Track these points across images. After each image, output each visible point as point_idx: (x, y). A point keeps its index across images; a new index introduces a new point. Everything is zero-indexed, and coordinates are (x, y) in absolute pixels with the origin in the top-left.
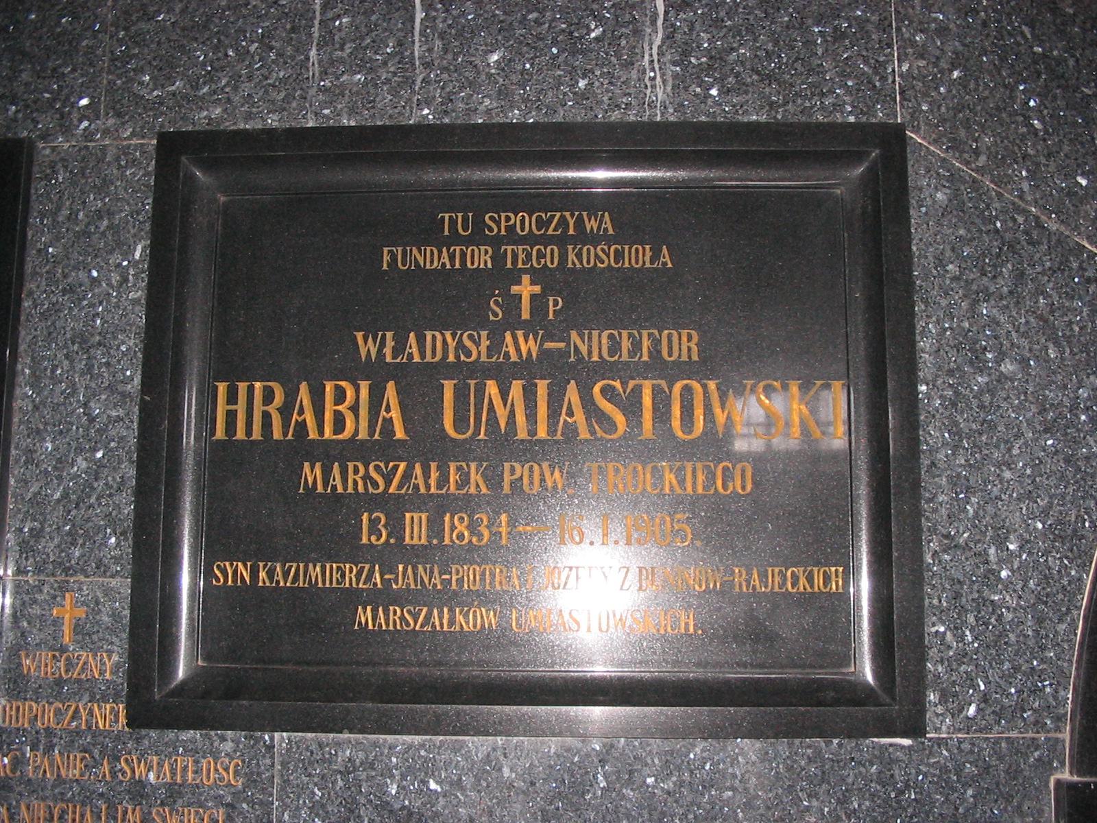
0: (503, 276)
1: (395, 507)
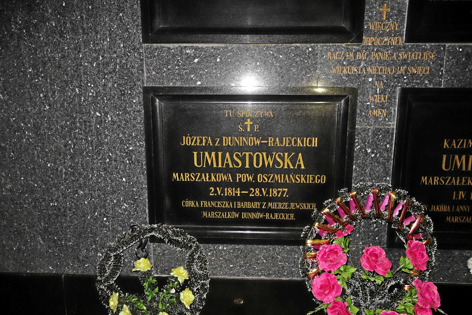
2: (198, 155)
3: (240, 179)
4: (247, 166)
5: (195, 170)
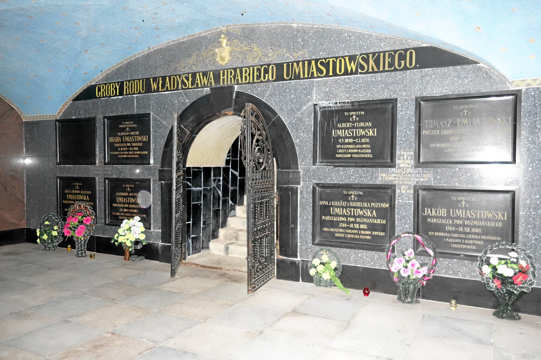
0: (126, 128)
1: (120, 147)
2: (333, 209)
3: (349, 220)
4: (352, 215)
5: (331, 215)
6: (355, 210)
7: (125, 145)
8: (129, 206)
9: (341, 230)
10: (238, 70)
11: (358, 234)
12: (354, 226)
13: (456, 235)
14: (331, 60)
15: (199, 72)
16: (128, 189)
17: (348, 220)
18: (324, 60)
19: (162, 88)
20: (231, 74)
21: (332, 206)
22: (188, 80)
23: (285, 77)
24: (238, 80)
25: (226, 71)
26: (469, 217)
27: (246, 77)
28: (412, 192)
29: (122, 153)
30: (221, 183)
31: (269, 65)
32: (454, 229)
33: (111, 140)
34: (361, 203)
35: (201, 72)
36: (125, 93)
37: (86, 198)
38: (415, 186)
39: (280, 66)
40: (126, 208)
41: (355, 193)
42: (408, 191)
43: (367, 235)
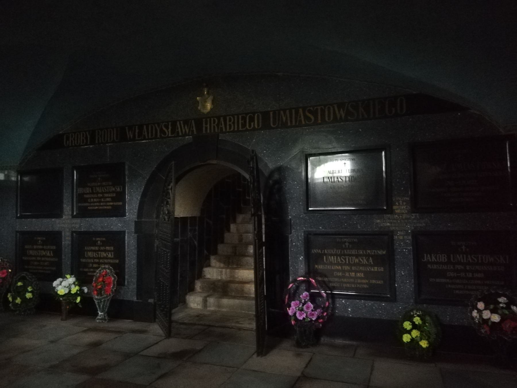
1: (91, 198)
3: (344, 268)
4: (347, 262)
6: (350, 258)
7: (96, 196)
8: (99, 261)
9: (336, 279)
10: (222, 119)
11: (354, 283)
12: (349, 274)
13: (458, 281)
14: (319, 108)
15: (180, 121)
16: (99, 242)
17: (343, 268)
18: (311, 108)
19: (139, 137)
20: (214, 123)
21: (325, 254)
22: (167, 128)
23: (272, 125)
24: (222, 128)
25: (208, 119)
26: (471, 261)
27: (230, 126)
28: (410, 238)
29: (92, 204)
30: (197, 233)
31: (254, 113)
32: (455, 275)
33: (81, 190)
34: (356, 250)
35: (182, 120)
36: (97, 142)
37: (50, 253)
38: (413, 232)
39: (265, 115)
40: (96, 263)
41: (349, 240)
42: (406, 237)
43: (364, 284)
